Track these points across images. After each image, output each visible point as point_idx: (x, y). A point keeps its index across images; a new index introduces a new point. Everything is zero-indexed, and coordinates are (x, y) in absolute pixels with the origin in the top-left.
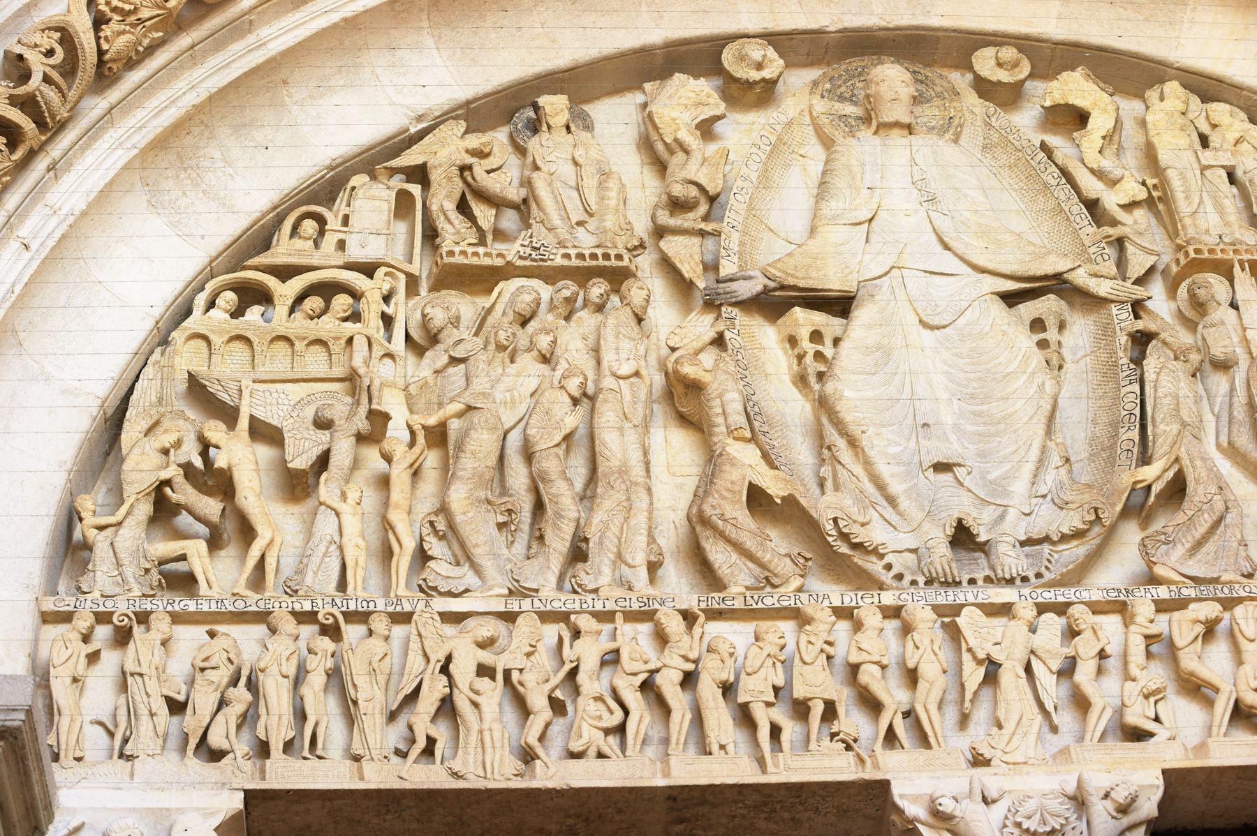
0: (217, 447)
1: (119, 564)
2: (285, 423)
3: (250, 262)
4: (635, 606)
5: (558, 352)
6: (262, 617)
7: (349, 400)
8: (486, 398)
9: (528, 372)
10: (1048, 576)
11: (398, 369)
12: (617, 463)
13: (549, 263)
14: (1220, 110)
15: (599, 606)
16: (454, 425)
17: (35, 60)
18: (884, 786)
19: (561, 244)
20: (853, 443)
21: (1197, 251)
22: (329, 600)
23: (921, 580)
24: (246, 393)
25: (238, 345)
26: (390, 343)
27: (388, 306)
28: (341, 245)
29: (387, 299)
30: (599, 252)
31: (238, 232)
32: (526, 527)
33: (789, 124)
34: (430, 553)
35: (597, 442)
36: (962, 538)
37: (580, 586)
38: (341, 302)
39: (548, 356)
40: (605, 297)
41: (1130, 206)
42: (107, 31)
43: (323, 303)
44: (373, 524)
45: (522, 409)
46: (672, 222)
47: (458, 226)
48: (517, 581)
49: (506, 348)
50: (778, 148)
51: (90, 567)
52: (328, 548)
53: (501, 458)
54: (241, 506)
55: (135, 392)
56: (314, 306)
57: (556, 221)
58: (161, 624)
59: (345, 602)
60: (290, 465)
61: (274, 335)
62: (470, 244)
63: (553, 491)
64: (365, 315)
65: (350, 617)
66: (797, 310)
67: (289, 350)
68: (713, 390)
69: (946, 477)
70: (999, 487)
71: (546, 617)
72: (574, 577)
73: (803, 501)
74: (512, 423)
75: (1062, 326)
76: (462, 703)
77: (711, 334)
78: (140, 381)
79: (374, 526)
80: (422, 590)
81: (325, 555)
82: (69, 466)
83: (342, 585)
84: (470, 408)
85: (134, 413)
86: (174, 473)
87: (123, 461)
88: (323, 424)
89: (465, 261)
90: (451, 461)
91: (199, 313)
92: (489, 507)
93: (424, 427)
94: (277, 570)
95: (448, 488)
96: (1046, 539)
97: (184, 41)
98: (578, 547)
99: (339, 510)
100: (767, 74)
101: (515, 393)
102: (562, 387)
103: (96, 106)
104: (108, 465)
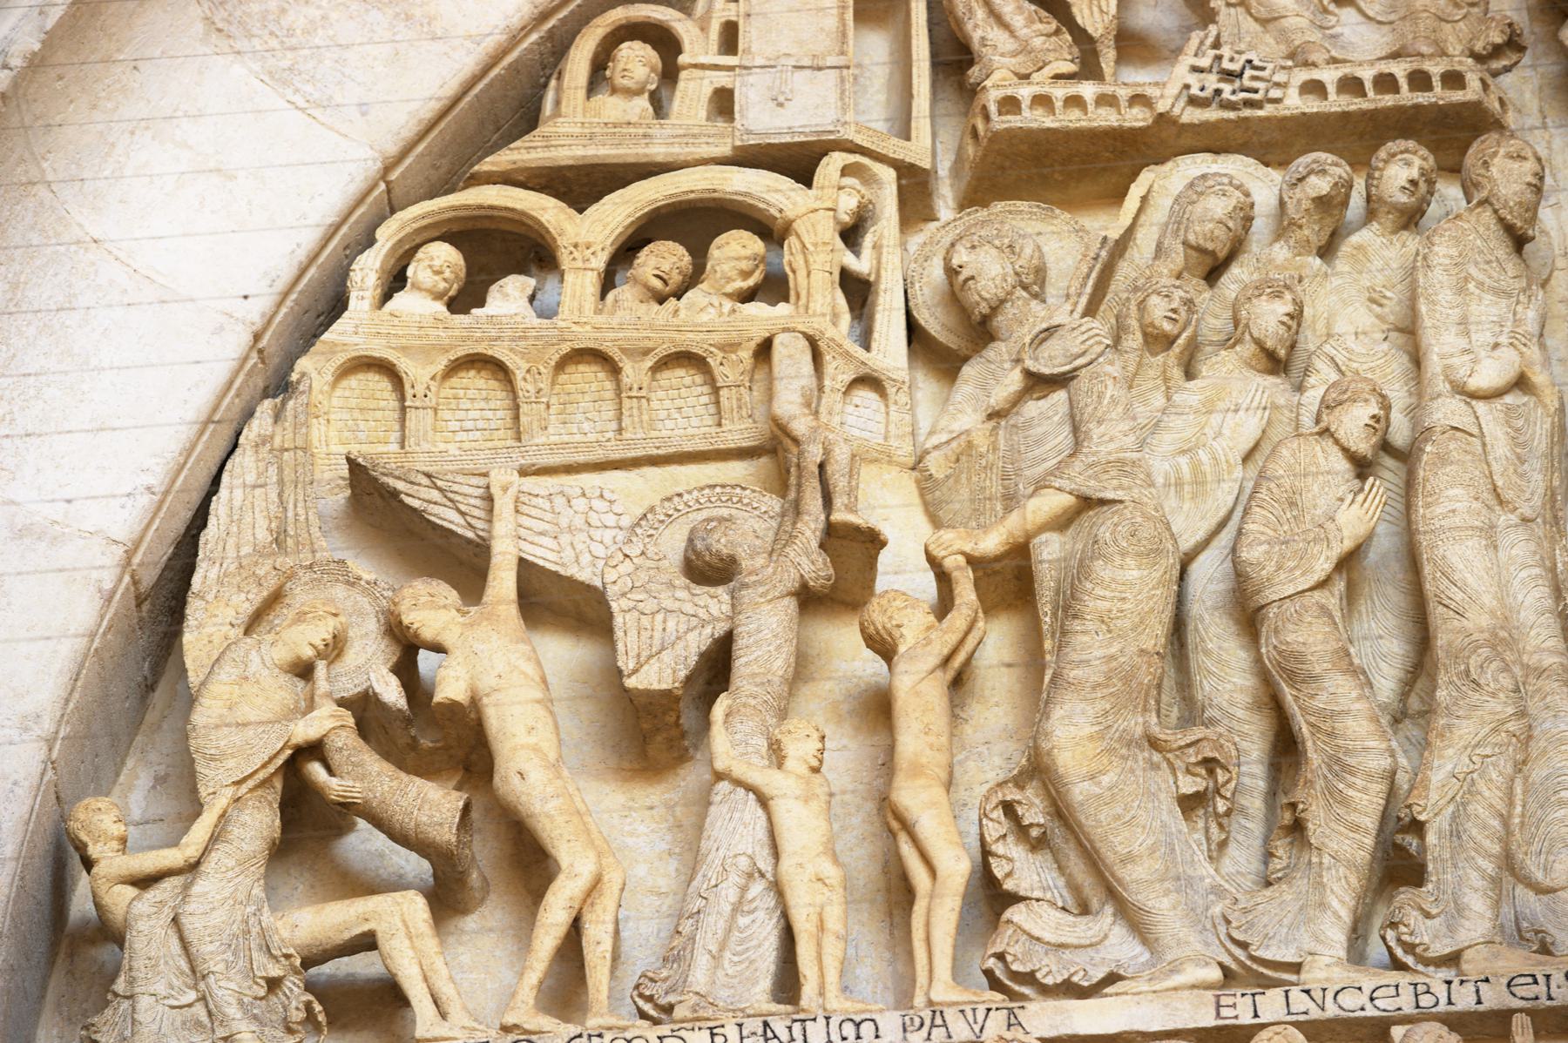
0: (438, 648)
1: (196, 973)
2: (611, 576)
3: (489, 164)
5: (1309, 340)
7: (773, 503)
8: (1127, 474)
11: (894, 416)
12: (1485, 621)
13: (1268, 110)
16: (1050, 550)
19: (1298, 57)
22: (755, 1025)
24: (503, 504)
25: (475, 382)
26: (867, 348)
27: (857, 254)
28: (723, 103)
29: (851, 235)
30: (1399, 70)
31: (451, 87)
32: (1255, 803)
34: (1009, 885)
35: (1427, 569)
37: (1410, 948)
39: (1282, 353)
40: (1423, 187)
43: (687, 258)
44: (856, 820)
45: (1222, 497)
47: (1023, 32)
48: (1244, 946)
49: (1169, 341)
51: (120, 986)
52: (744, 889)
53: (1179, 627)
54: (511, 798)
55: (212, 521)
56: (666, 267)
59: (797, 1027)
60: (631, 683)
61: (566, 348)
62: (1058, 77)
63: (1319, 703)
64: (798, 281)
67: (609, 385)
72: (1393, 925)
74: (1200, 535)
78: (223, 492)
79: (859, 822)
80: (995, 984)
81: (737, 909)
82: (47, 726)
84: (1087, 503)
85: (213, 573)
86: (330, 724)
87: (191, 701)
89: (1049, 122)
90: (1048, 645)
91: (366, 305)
92: (1157, 757)
93: (972, 561)
94: (616, 957)
95: (1046, 715)
98: (1400, 849)
99: (766, 790)
101: (1203, 455)
102: (1326, 432)
104: (151, 717)
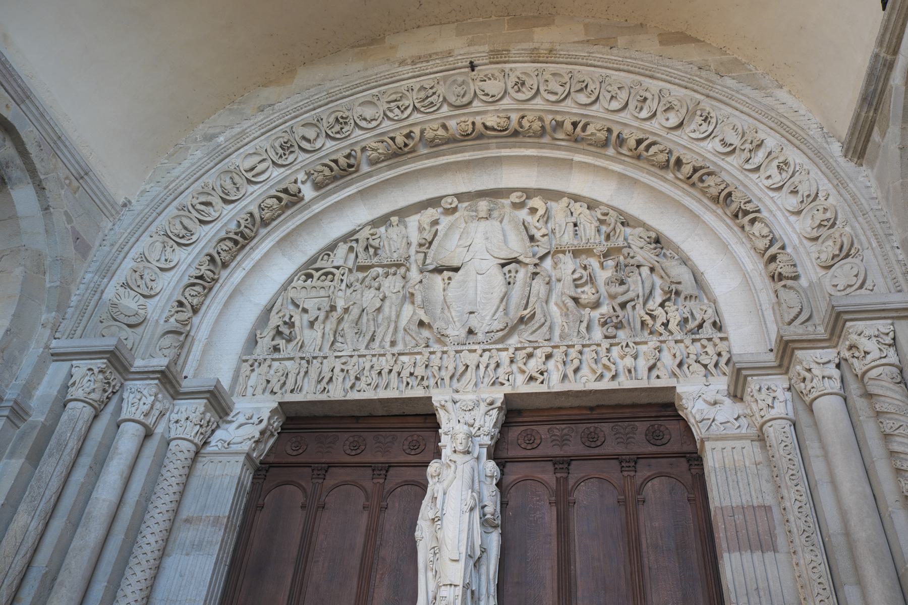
6: (292, 359)
10: (489, 341)
14: (578, 204)
17: (243, 223)
18: (431, 398)
20: (448, 308)
25: (304, 289)
29: (343, 275)
36: (471, 332)
38: (330, 277)
41: (543, 236)
46: (418, 250)
50: (451, 227)
57: (388, 252)
58: (268, 362)
68: (415, 295)
69: (472, 315)
70: (483, 318)
71: (360, 356)
73: (431, 324)
75: (517, 272)
76: (334, 379)
77: (419, 280)
88: (319, 309)
96: (493, 332)
97: (289, 212)
100: (453, 206)
103: (263, 231)
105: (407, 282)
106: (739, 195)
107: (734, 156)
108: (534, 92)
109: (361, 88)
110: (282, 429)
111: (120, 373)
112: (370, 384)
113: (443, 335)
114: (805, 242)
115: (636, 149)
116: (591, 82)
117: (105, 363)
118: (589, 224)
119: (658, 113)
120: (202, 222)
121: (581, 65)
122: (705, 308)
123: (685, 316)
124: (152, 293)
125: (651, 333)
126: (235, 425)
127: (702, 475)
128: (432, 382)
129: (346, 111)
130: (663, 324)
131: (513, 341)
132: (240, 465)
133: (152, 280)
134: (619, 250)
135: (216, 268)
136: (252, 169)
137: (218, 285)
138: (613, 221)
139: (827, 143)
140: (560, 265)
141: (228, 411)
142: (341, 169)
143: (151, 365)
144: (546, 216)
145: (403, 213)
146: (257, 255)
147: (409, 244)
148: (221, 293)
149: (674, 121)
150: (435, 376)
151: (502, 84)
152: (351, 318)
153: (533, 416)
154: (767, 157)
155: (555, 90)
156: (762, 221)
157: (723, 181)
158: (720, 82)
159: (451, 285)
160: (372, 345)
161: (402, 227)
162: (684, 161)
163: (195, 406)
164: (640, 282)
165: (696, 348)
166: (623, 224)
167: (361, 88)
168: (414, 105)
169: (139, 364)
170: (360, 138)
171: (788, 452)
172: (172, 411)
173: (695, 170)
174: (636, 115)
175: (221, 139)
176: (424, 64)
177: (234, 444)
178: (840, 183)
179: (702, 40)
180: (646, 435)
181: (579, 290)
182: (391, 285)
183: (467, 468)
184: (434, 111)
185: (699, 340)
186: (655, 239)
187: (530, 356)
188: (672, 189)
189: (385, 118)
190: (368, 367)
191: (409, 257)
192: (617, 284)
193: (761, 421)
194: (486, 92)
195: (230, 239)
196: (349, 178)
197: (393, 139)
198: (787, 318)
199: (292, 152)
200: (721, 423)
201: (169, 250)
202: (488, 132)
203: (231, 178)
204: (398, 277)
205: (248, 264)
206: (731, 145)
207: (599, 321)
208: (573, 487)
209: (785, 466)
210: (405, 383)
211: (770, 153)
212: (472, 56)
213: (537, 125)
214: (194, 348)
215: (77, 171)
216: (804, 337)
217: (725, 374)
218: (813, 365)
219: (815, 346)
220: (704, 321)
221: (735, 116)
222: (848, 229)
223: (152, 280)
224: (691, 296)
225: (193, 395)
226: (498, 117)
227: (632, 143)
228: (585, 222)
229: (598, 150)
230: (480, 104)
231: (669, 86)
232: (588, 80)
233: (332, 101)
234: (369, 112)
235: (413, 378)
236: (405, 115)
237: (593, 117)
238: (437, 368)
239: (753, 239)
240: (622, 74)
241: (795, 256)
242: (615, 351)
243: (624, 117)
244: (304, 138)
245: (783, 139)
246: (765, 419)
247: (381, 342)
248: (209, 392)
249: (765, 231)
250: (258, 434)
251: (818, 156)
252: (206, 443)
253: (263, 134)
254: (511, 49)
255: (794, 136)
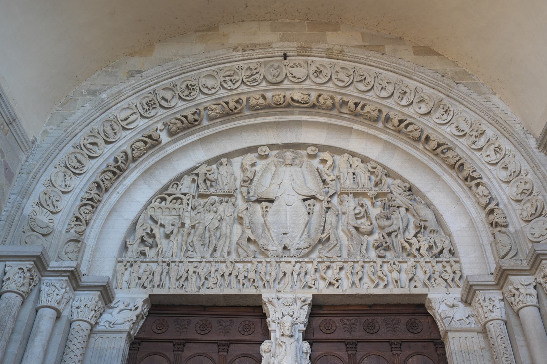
1: (133, 252)
4: (223, 260)
6: (157, 262)
9: (211, 215)
10: (299, 256)
14: (355, 159)
15: (217, 260)
16: (197, 225)
17: (120, 159)
18: (261, 295)
20: (268, 229)
21: (342, 190)
23: (276, 256)
25: (160, 209)
28: (181, 189)
29: (188, 200)
30: (228, 191)
33: (269, 164)
36: (285, 248)
38: (179, 201)
42: (134, 152)
46: (243, 185)
50: (266, 169)
57: (221, 185)
58: (138, 263)
65: (172, 262)
66: (263, 202)
68: (244, 218)
69: (285, 236)
70: (294, 238)
71: (206, 262)
73: (257, 241)
75: (314, 205)
76: (189, 278)
77: (246, 208)
83: (172, 256)
84: (200, 222)
88: (173, 225)
94: (161, 252)
96: (301, 249)
97: (151, 152)
100: (266, 153)
103: (133, 165)
105: (235, 208)
106: (468, 166)
107: (464, 138)
108: (328, 78)
109: (205, 65)
110: (149, 314)
111: (39, 271)
112: (216, 283)
113: (266, 249)
114: (512, 202)
115: (398, 126)
116: (368, 76)
117: (32, 264)
118: (363, 175)
119: (414, 103)
120: (90, 157)
121: (362, 63)
122: (444, 239)
123: (431, 244)
124: (58, 210)
125: (408, 255)
126: (117, 310)
127: (444, 354)
128: (260, 284)
129: (194, 81)
130: (417, 249)
131: (315, 255)
132: (124, 340)
133: (57, 201)
134: (385, 194)
135: (101, 193)
136: (126, 119)
137: (101, 205)
138: (380, 173)
139: (527, 137)
140: (346, 203)
141: (112, 299)
142: (189, 123)
143: (63, 266)
144: (333, 166)
145: (229, 156)
146: (128, 182)
147: (235, 179)
148: (104, 210)
149: (424, 109)
150: (262, 280)
151: (306, 71)
152: (198, 233)
153: (330, 310)
154: (487, 143)
155: (343, 79)
156: (483, 185)
157: (458, 155)
158: (456, 87)
159: (269, 213)
160: (215, 254)
161: (229, 166)
162: (432, 138)
163: (91, 296)
164: (400, 220)
165: (439, 267)
166: (386, 175)
167: (205, 65)
168: (242, 80)
169: (53, 264)
170: (202, 101)
171: (503, 342)
172: (74, 300)
173: (439, 145)
174: (399, 102)
175: (104, 96)
176: (251, 52)
177: (117, 324)
178: (535, 166)
179: (442, 54)
180: (407, 326)
181: (359, 222)
182: (225, 210)
183: (293, 347)
184: (256, 85)
185: (441, 262)
186: (409, 188)
187: (328, 267)
188: (422, 155)
189: (221, 88)
190: (213, 269)
191: (237, 189)
192: (385, 219)
193: (485, 320)
194: (294, 75)
195: (110, 171)
196: (194, 128)
197: (227, 103)
198: (502, 254)
199: (154, 108)
200: (458, 320)
201: (68, 178)
202: (295, 104)
203: (111, 125)
204: (230, 204)
205: (121, 189)
206: (463, 131)
207: (374, 245)
208: (360, 361)
209: (502, 352)
210: (242, 284)
211: (489, 140)
212: (285, 49)
213: (329, 102)
214: (86, 251)
215: (8, 118)
216: (515, 268)
217: (458, 286)
218: (520, 287)
219: (521, 273)
220: (443, 249)
221: (466, 111)
222: (540, 197)
223: (57, 201)
224: (434, 231)
225: (90, 288)
226: (302, 93)
227: (396, 122)
228: (360, 173)
229: (371, 123)
230: (289, 83)
231: (421, 85)
232: (366, 74)
233: (184, 73)
234: (210, 83)
235: (246, 280)
236: (236, 86)
237: (368, 100)
238: (264, 274)
239: (478, 197)
240: (390, 73)
241: (505, 211)
242: (386, 266)
243: (390, 103)
244: (163, 98)
245: (498, 132)
246: (488, 319)
247: (221, 252)
248: (102, 286)
249: (486, 193)
250: (136, 317)
251: (521, 146)
252: (97, 323)
253: (134, 94)
254: (313, 47)
255: (505, 130)
